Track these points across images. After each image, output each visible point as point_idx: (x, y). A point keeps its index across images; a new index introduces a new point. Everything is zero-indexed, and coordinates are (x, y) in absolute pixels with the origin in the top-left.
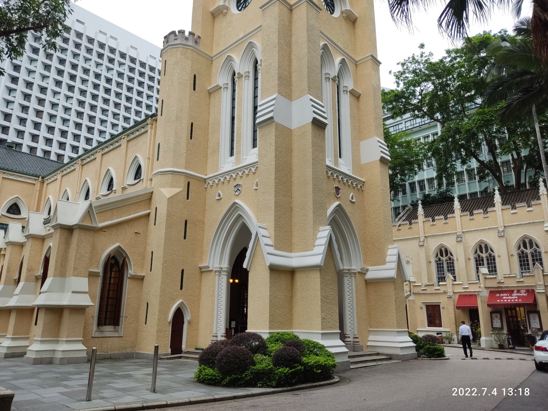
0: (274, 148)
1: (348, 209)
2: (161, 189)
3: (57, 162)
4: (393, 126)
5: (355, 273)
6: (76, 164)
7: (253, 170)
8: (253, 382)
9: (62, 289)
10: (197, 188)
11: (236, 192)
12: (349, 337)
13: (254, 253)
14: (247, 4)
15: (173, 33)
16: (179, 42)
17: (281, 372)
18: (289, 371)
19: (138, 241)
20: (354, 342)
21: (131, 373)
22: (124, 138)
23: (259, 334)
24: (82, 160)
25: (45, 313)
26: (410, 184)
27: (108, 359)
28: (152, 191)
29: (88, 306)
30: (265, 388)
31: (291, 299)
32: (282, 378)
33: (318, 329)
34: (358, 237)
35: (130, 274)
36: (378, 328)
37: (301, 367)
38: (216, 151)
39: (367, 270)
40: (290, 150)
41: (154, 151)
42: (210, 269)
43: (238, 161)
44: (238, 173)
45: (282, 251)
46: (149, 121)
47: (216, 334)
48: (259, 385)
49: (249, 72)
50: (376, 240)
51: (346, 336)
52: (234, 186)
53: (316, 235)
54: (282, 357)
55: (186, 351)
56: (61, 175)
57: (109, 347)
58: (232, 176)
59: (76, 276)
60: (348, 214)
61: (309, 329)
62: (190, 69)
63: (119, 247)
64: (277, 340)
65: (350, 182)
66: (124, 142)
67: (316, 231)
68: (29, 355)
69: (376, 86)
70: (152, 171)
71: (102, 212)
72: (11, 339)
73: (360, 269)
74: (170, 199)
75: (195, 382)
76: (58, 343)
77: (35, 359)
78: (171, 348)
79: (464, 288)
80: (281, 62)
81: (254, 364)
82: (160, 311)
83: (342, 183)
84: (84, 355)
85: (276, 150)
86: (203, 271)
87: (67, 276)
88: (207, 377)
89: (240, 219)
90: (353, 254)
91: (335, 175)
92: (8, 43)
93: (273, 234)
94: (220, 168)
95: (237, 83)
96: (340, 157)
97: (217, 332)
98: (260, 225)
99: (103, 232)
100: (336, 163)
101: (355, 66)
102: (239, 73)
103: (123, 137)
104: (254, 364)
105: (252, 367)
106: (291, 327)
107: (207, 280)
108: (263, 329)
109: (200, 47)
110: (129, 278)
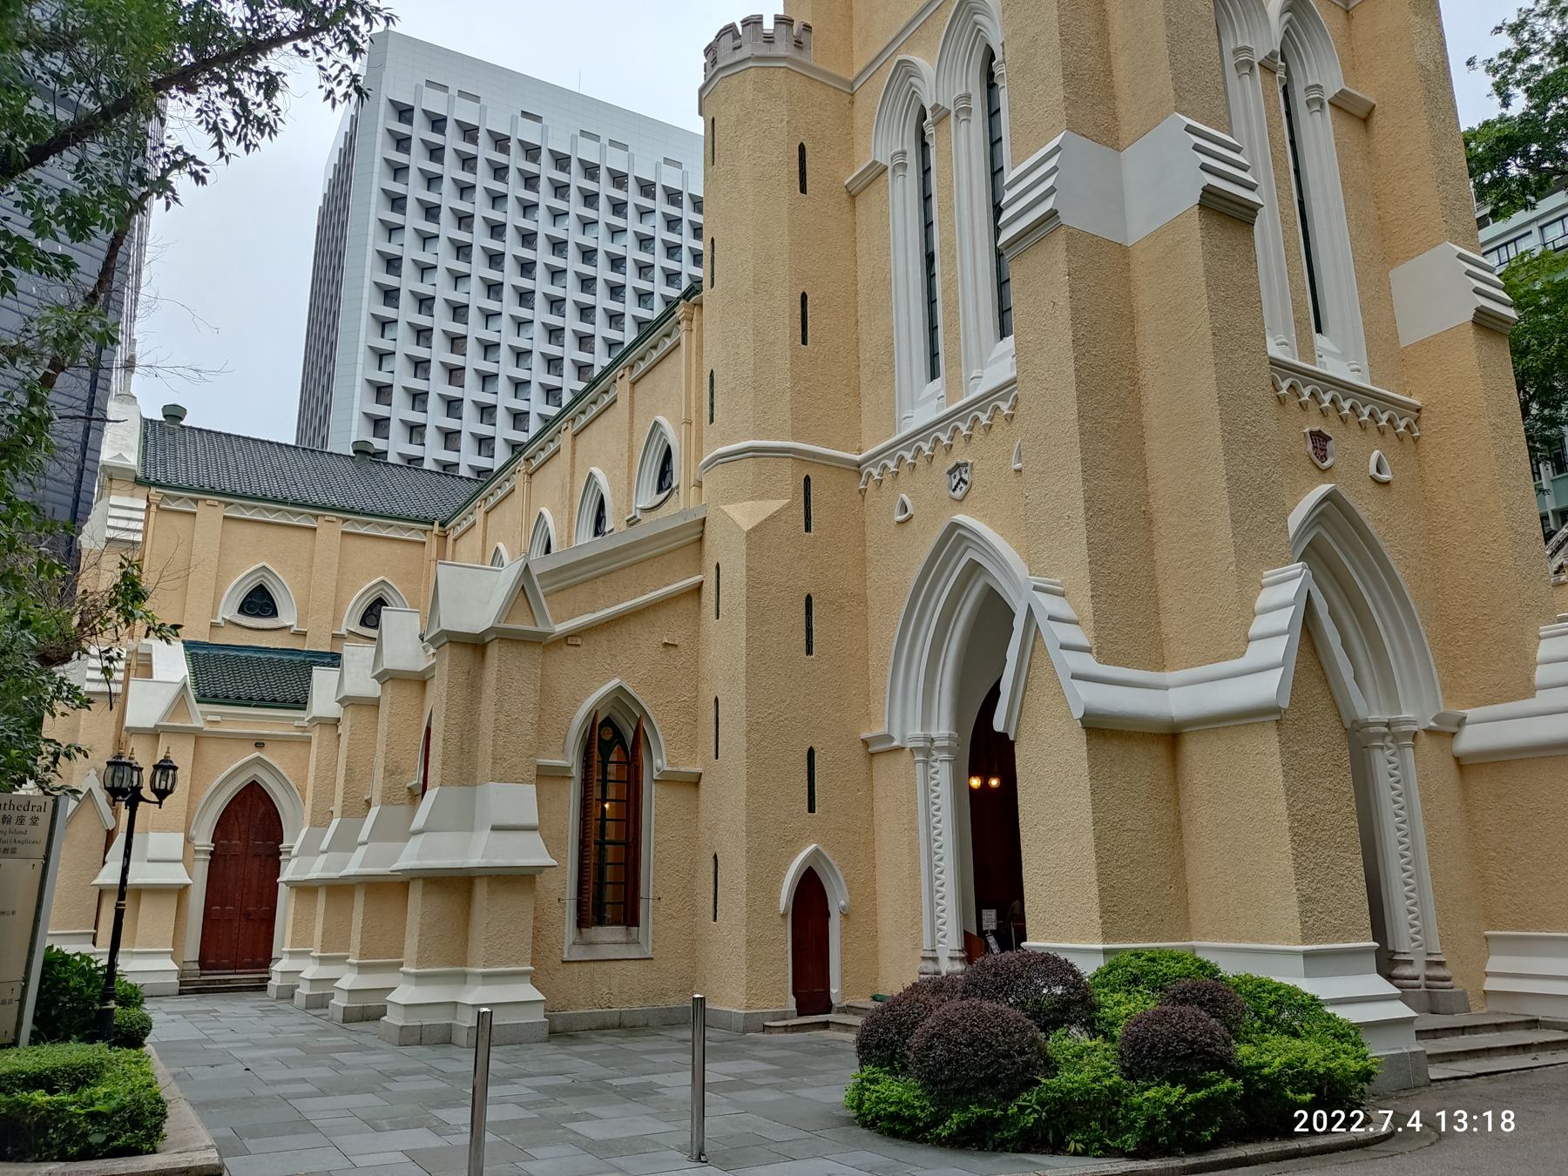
0: (1067, 313)
1: (1367, 507)
2: (726, 508)
3: (476, 481)
4: (1497, 248)
5: (1416, 733)
6: (514, 473)
8: (1051, 1134)
9: (466, 823)
10: (835, 495)
11: (954, 490)
12: (1410, 962)
13: (1027, 678)
15: (730, 29)
16: (748, 54)
17: (1155, 1102)
18: (1184, 1096)
19: (674, 671)
20: (1428, 978)
21: (656, 1079)
22: (623, 375)
23: (1062, 957)
24: (527, 460)
25: (423, 894)
27: (613, 1028)
28: (702, 517)
29: (542, 868)
30: (1097, 1157)
31: (1175, 831)
32: (1159, 1122)
33: (1288, 939)
34: (1413, 606)
35: (658, 770)
36: (1523, 929)
37: (1234, 1081)
38: (886, 369)
39: (1461, 722)
40: (1127, 319)
41: (699, 398)
42: (895, 743)
43: (953, 389)
44: (956, 429)
45: (1126, 666)
46: (680, 311)
47: (934, 950)
48: (1072, 1146)
49: (968, 97)
50: (1487, 611)
51: (1396, 957)
52: (946, 470)
53: (1253, 599)
54: (1153, 1046)
55: (844, 1004)
56: (483, 509)
57: (615, 991)
58: (937, 440)
59: (501, 780)
60: (1370, 525)
61: (1253, 940)
62: (785, 130)
63: (620, 688)
64: (1135, 980)
65: (1366, 411)
66: (622, 389)
67: (1249, 586)
68: (393, 1018)
69: (1432, 67)
70: (699, 459)
71: (563, 589)
72: (356, 970)
73: (1434, 720)
74: (752, 535)
75: (850, 1122)
76: (465, 983)
77: (402, 1027)
78: (795, 993)
80: (1068, 26)
81: (1051, 1068)
82: (750, 879)
83: (1332, 415)
84: (538, 1016)
85: (1076, 320)
86: (875, 751)
87: (478, 781)
88: (885, 1109)
89: (974, 578)
90: (1399, 667)
91: (1307, 392)
92: (234, 103)
93: (1088, 609)
94: (900, 422)
95: (932, 143)
96: (1319, 330)
97: (933, 944)
98: (1036, 580)
99: (570, 648)
100: (1307, 350)
101: (1341, 15)
102: (936, 107)
103: (619, 375)
104: (1051, 1068)
105: (1044, 1081)
106: (1185, 931)
107: (888, 774)
108: (1082, 937)
109: (810, 58)
110: (656, 780)
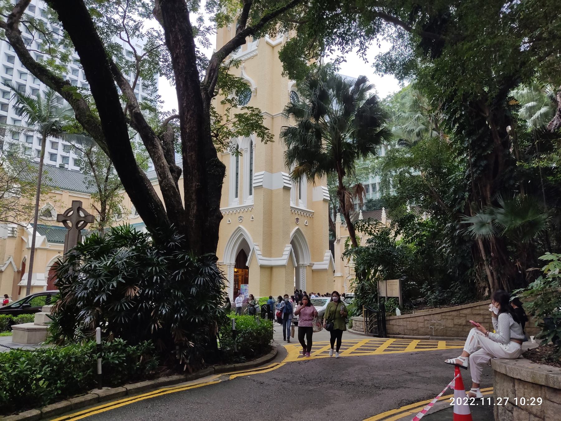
7: (250, 209)
14: (246, 102)
26: (366, 186)
31: (271, 281)
39: (313, 264)
43: (241, 202)
83: (300, 215)
93: (262, 248)
96: (300, 199)
98: (255, 244)
100: (297, 204)
102: (241, 148)
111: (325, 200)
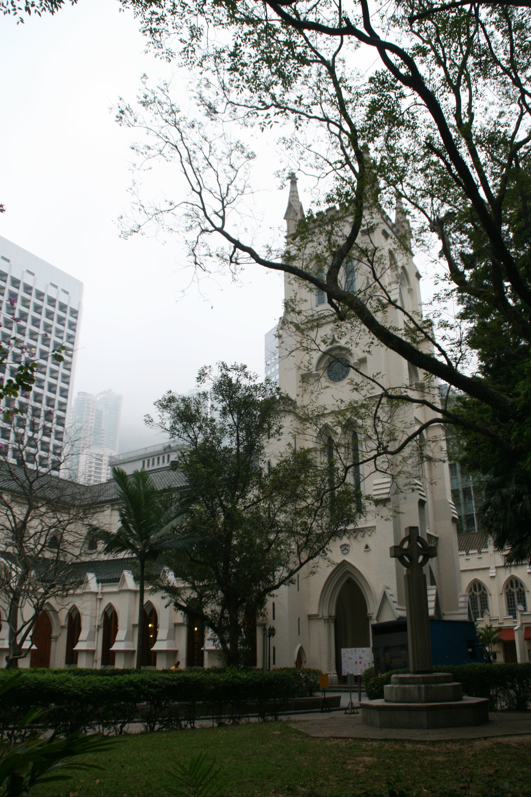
79: (500, 623)
111: (454, 519)
